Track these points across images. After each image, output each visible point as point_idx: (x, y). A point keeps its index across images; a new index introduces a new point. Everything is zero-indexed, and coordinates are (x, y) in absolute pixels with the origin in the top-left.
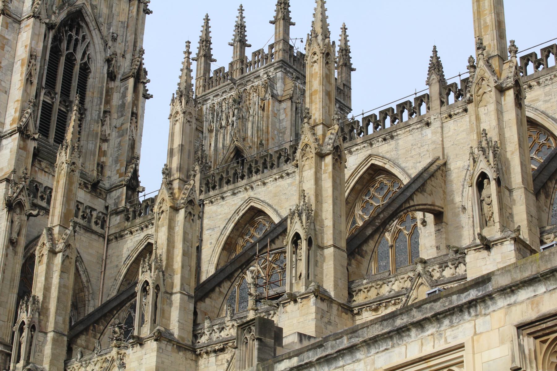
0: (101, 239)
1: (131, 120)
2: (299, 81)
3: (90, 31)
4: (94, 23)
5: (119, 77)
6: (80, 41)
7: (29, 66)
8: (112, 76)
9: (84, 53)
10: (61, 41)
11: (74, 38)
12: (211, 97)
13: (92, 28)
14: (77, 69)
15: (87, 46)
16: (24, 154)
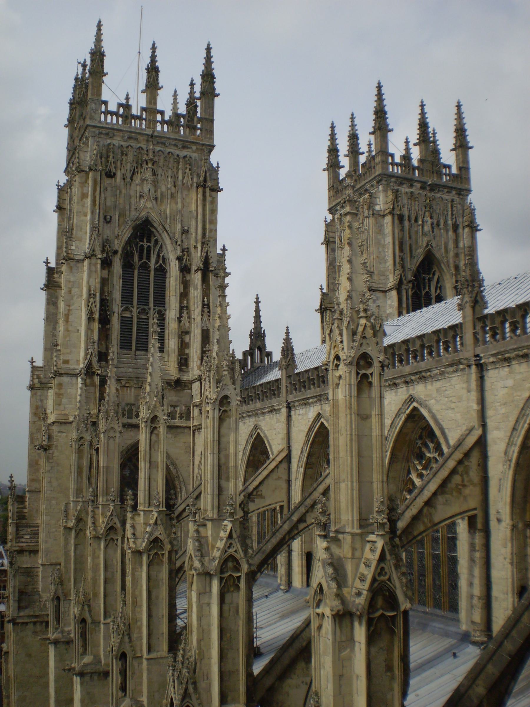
0: (186, 430)
1: (203, 311)
2: (405, 186)
3: (160, 234)
4: (161, 227)
5: (194, 268)
6: (152, 247)
7: (88, 306)
8: (185, 270)
9: (158, 256)
10: (133, 255)
11: (145, 247)
12: (338, 208)
13: (161, 232)
14: (152, 273)
15: (161, 247)
16: (92, 389)
